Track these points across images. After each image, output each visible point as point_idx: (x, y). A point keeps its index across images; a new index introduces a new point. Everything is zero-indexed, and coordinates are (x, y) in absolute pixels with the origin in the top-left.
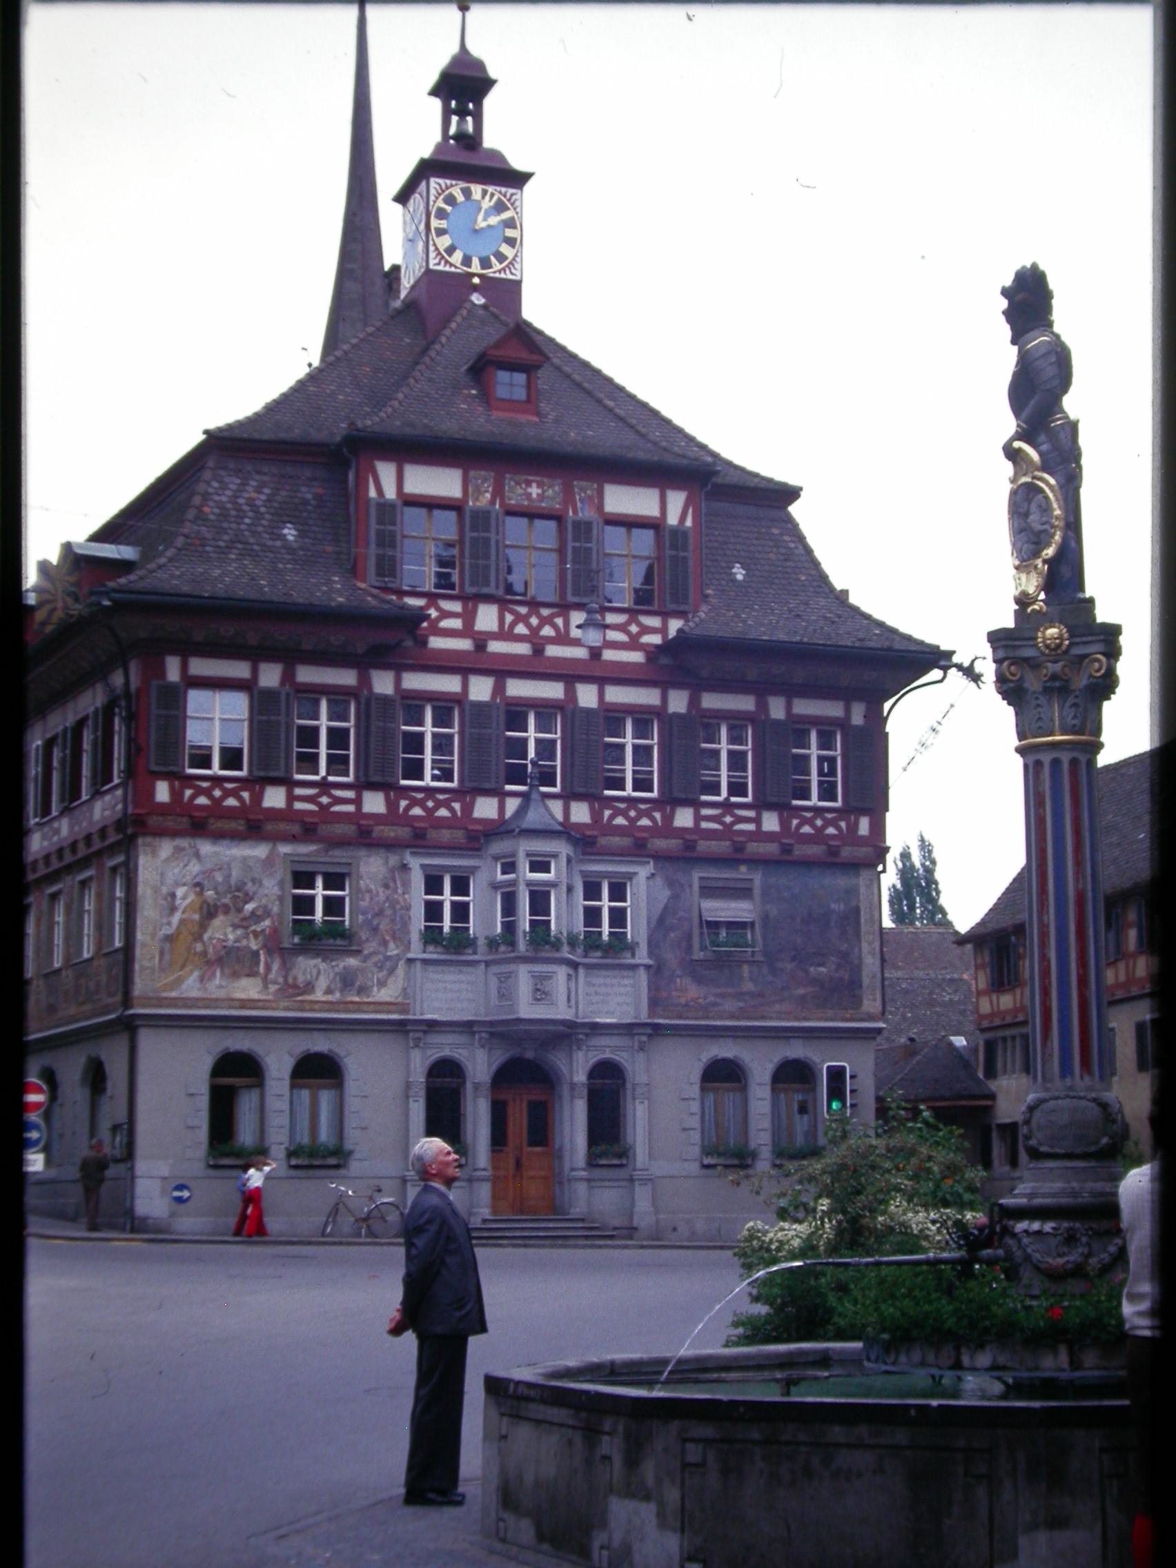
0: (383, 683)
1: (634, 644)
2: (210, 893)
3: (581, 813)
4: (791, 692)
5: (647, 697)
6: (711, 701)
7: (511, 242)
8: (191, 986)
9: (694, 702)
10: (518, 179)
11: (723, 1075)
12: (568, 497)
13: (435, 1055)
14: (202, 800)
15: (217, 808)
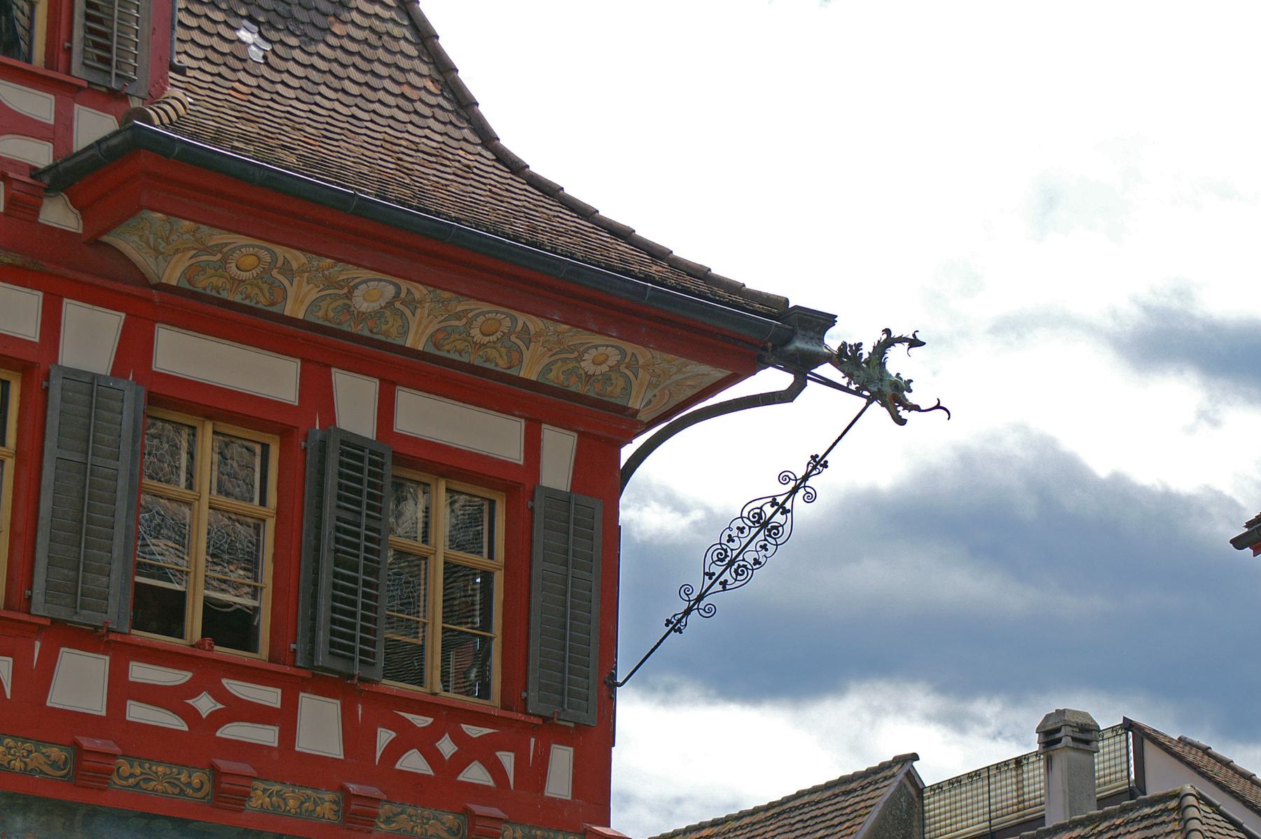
4: (396, 368)
9: (134, 350)
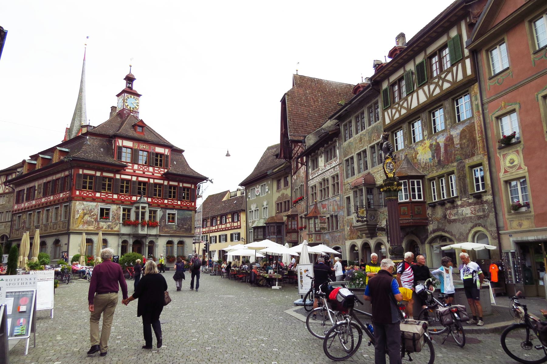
0: (118, 176)
1: (159, 173)
2: (85, 211)
3: (150, 200)
5: (161, 182)
6: (171, 183)
7: (138, 105)
8: (81, 227)
9: (168, 183)
10: (139, 95)
11: (170, 243)
12: (150, 148)
13: (123, 239)
14: (85, 195)
15: (87, 196)
